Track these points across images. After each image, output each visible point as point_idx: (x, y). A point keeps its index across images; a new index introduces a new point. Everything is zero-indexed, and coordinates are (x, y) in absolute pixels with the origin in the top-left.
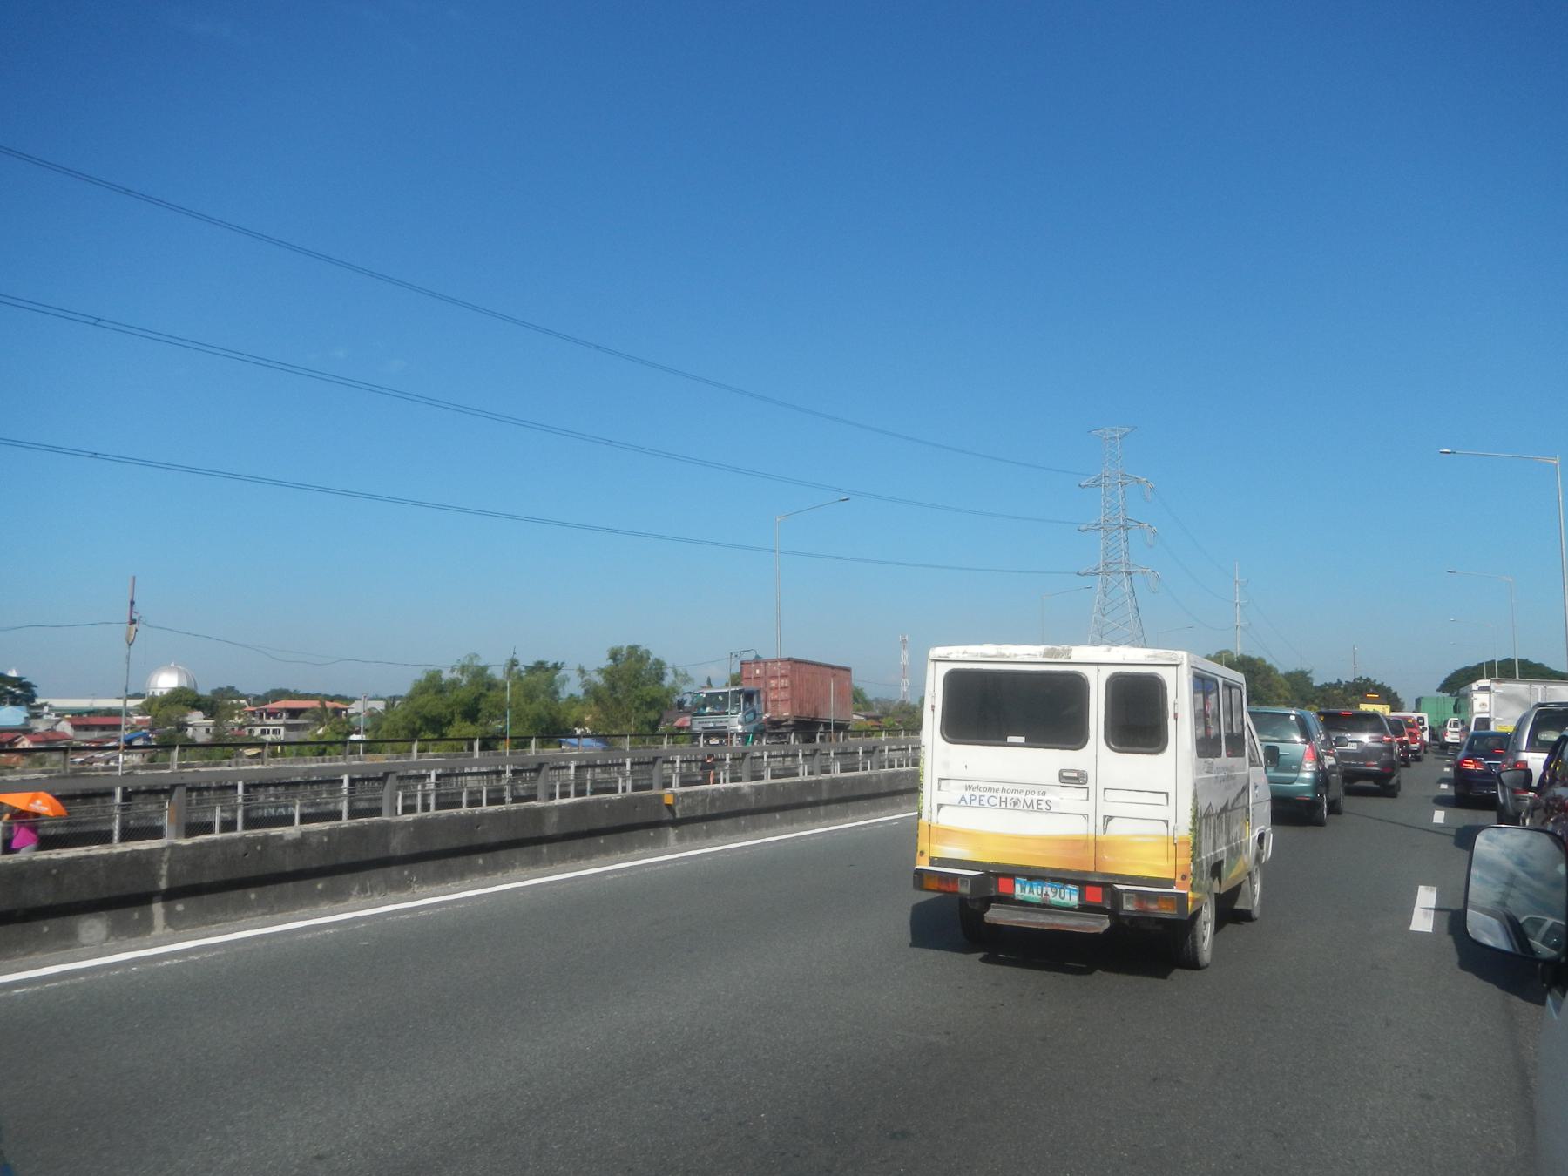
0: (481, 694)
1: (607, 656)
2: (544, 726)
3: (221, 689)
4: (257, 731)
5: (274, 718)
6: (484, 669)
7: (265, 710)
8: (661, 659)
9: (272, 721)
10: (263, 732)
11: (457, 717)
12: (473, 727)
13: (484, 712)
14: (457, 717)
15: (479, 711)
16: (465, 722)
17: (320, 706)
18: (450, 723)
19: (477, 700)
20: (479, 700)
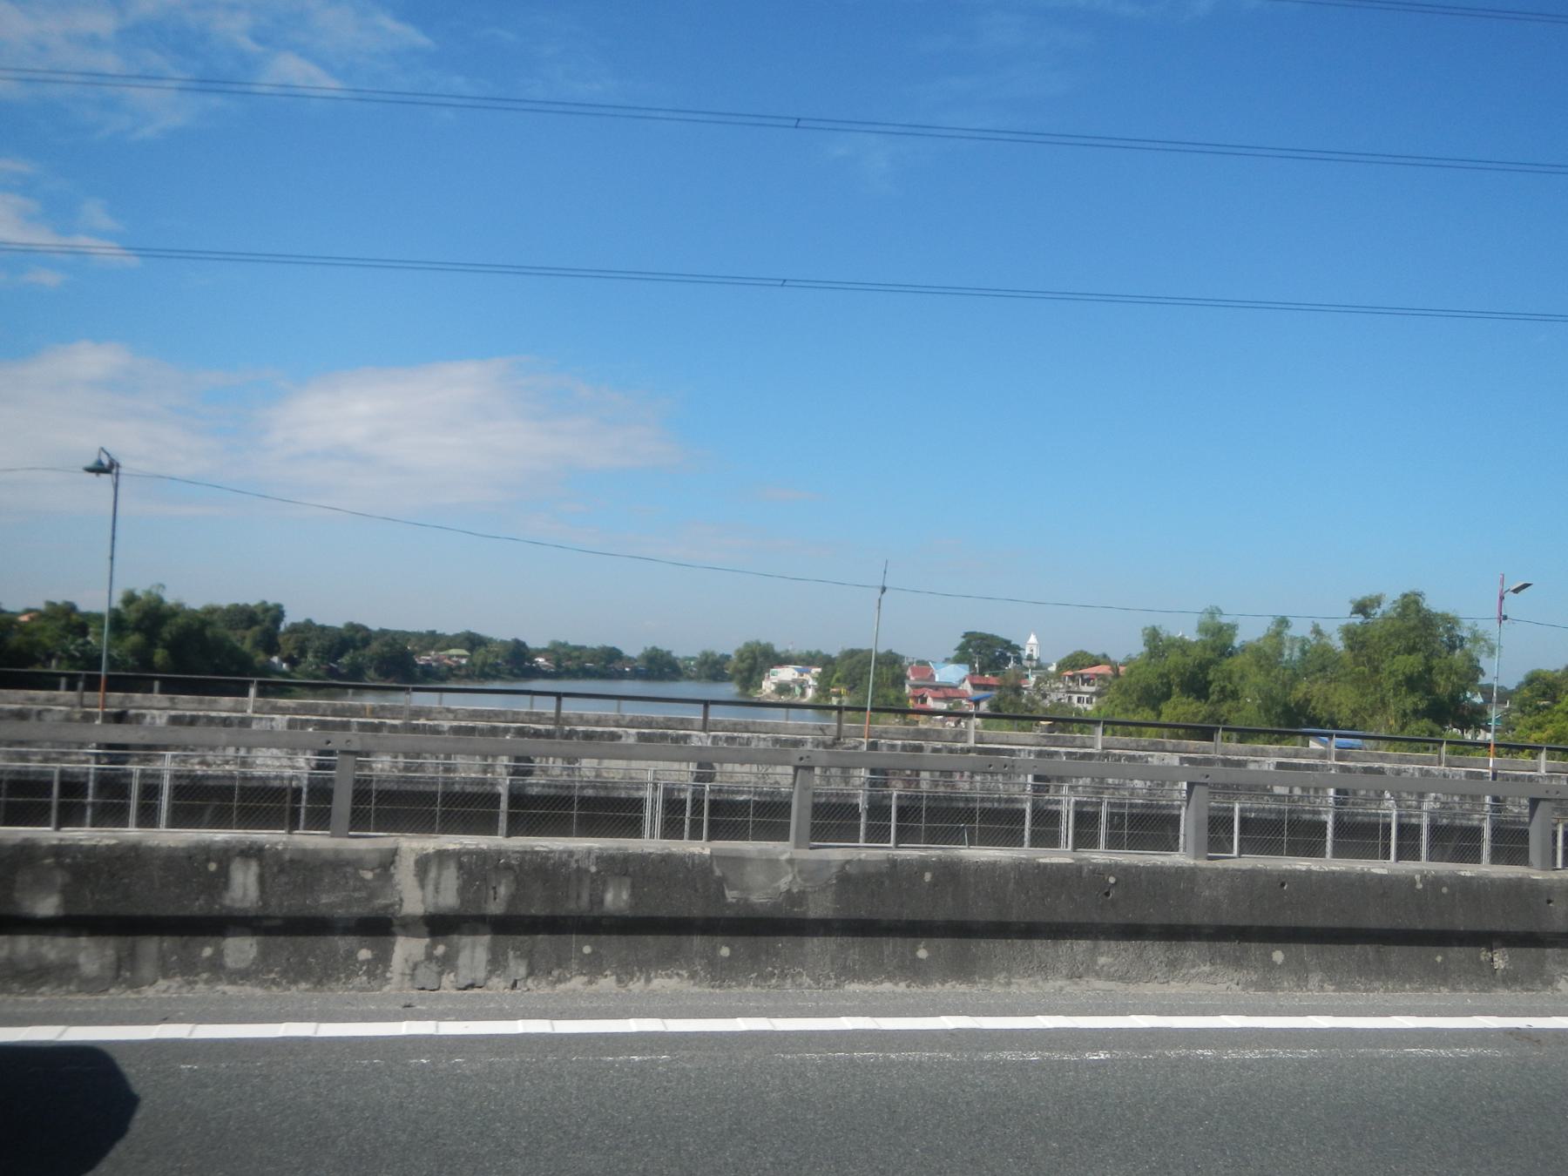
0: (1210, 662)
1: (1350, 608)
2: (1279, 710)
3: (1086, 653)
4: (1075, 698)
5: (1088, 685)
6: (1233, 628)
7: (1082, 675)
8: (1452, 614)
9: (1085, 688)
10: (1079, 699)
11: (1176, 689)
12: (1198, 704)
13: (1214, 688)
14: (1176, 689)
15: (1210, 683)
16: (1188, 697)
17: (1110, 672)
18: (1167, 696)
19: (1204, 666)
20: (1208, 668)
